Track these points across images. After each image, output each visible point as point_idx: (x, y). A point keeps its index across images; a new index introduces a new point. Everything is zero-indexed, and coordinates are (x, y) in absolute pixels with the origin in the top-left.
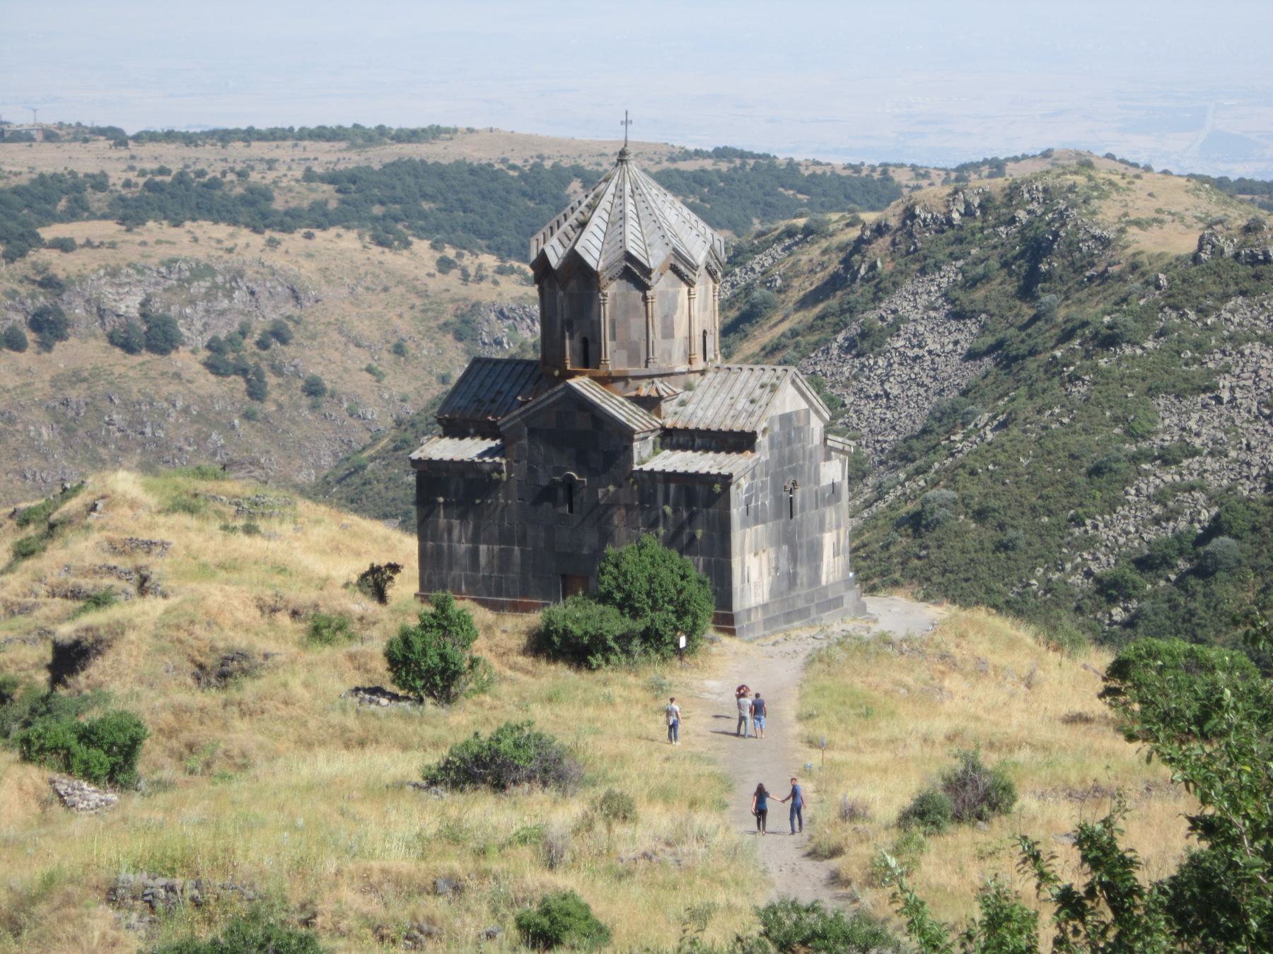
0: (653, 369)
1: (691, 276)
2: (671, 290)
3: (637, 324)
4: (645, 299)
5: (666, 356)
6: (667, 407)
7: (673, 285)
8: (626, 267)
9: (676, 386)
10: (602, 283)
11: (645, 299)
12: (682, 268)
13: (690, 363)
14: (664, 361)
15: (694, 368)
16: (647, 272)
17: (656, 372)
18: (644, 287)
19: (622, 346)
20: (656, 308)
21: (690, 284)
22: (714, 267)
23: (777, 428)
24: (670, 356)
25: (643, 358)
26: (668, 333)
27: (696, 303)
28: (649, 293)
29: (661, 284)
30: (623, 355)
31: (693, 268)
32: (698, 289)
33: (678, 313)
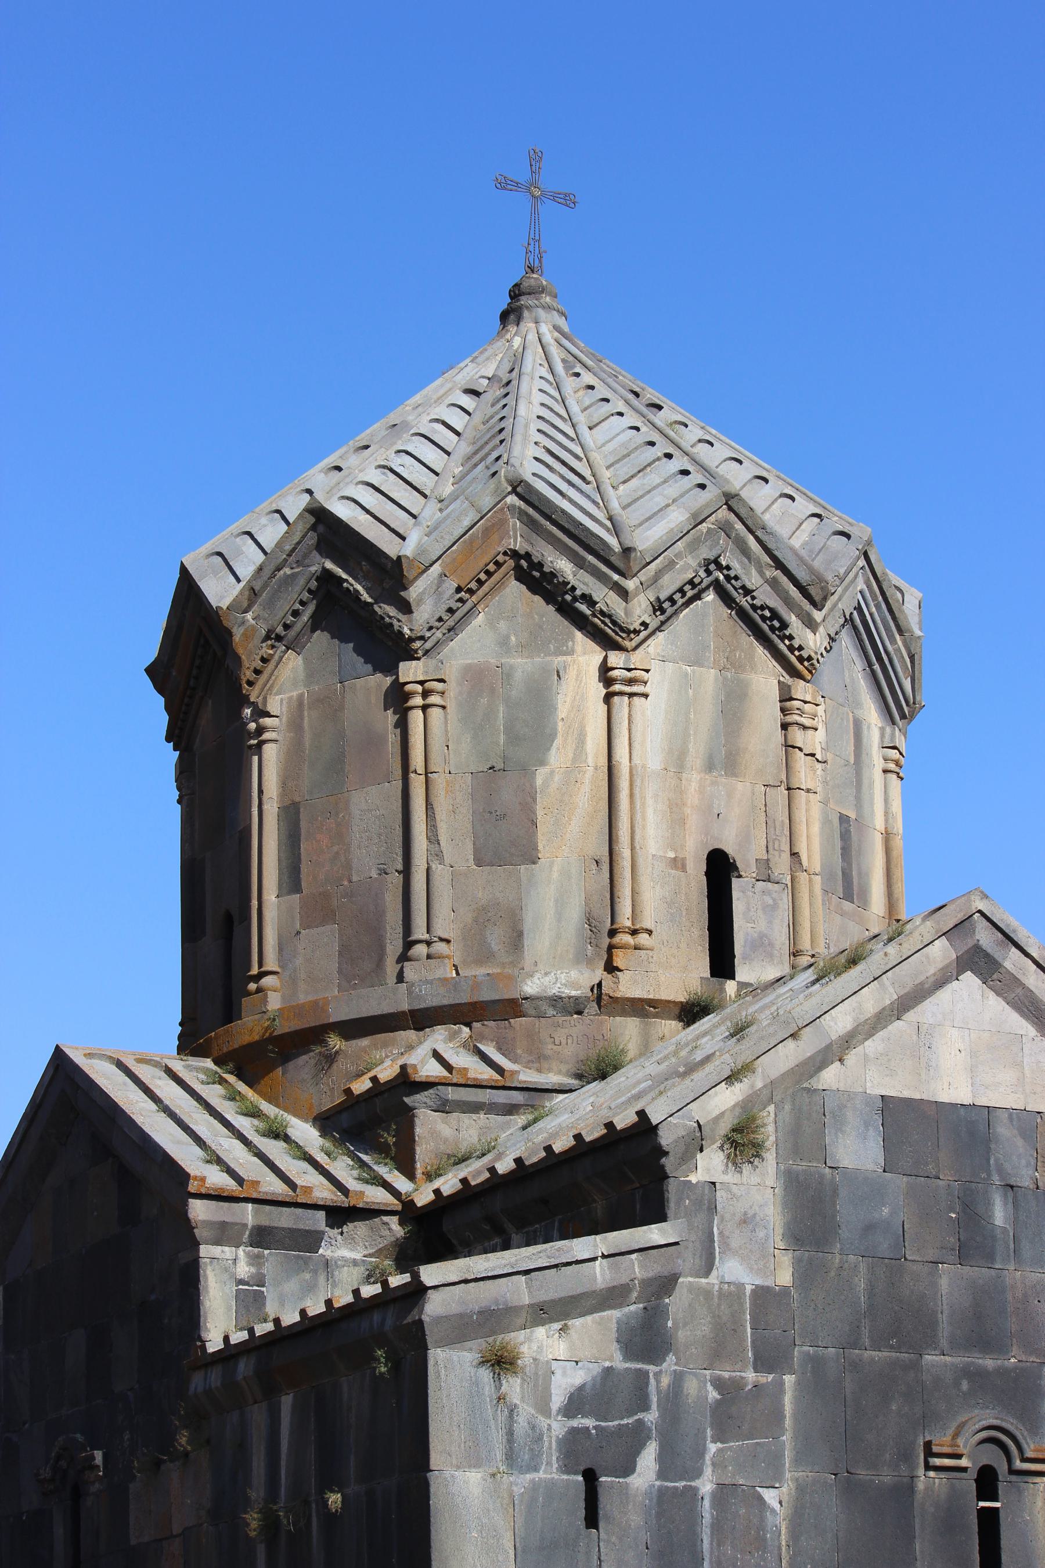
0: (429, 981)
1: (606, 599)
2: (522, 665)
3: (370, 805)
4: (398, 699)
5: (496, 938)
6: (433, 1129)
7: (534, 643)
8: (326, 576)
9: (538, 1059)
10: (249, 662)
11: (398, 699)
12: (564, 567)
13: (611, 968)
14: (485, 956)
15: (629, 985)
16: (390, 576)
17: (433, 998)
18: (387, 649)
19: (319, 911)
20: (442, 735)
21: (608, 635)
22: (765, 596)
23: (857, 1151)
24: (516, 940)
25: (393, 947)
26: (508, 840)
27: (650, 719)
28: (410, 671)
29: (481, 646)
30: (324, 944)
31: (616, 563)
32: (657, 660)
33: (558, 757)
